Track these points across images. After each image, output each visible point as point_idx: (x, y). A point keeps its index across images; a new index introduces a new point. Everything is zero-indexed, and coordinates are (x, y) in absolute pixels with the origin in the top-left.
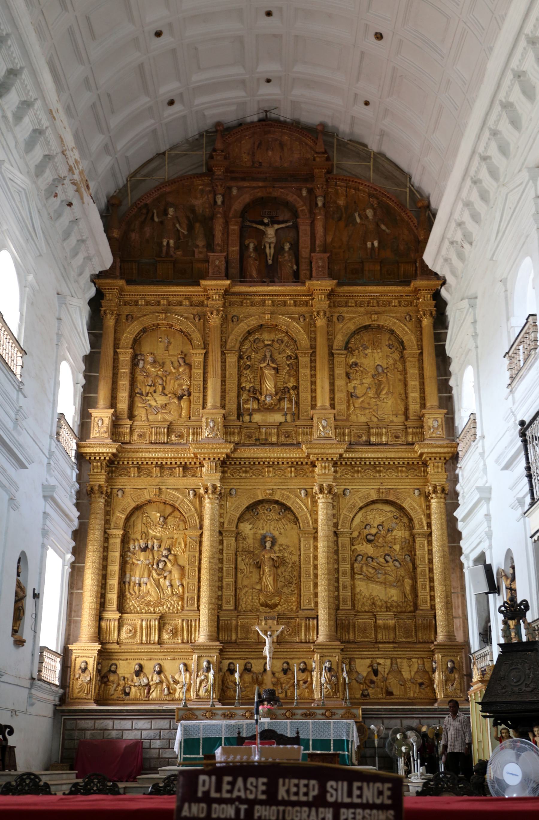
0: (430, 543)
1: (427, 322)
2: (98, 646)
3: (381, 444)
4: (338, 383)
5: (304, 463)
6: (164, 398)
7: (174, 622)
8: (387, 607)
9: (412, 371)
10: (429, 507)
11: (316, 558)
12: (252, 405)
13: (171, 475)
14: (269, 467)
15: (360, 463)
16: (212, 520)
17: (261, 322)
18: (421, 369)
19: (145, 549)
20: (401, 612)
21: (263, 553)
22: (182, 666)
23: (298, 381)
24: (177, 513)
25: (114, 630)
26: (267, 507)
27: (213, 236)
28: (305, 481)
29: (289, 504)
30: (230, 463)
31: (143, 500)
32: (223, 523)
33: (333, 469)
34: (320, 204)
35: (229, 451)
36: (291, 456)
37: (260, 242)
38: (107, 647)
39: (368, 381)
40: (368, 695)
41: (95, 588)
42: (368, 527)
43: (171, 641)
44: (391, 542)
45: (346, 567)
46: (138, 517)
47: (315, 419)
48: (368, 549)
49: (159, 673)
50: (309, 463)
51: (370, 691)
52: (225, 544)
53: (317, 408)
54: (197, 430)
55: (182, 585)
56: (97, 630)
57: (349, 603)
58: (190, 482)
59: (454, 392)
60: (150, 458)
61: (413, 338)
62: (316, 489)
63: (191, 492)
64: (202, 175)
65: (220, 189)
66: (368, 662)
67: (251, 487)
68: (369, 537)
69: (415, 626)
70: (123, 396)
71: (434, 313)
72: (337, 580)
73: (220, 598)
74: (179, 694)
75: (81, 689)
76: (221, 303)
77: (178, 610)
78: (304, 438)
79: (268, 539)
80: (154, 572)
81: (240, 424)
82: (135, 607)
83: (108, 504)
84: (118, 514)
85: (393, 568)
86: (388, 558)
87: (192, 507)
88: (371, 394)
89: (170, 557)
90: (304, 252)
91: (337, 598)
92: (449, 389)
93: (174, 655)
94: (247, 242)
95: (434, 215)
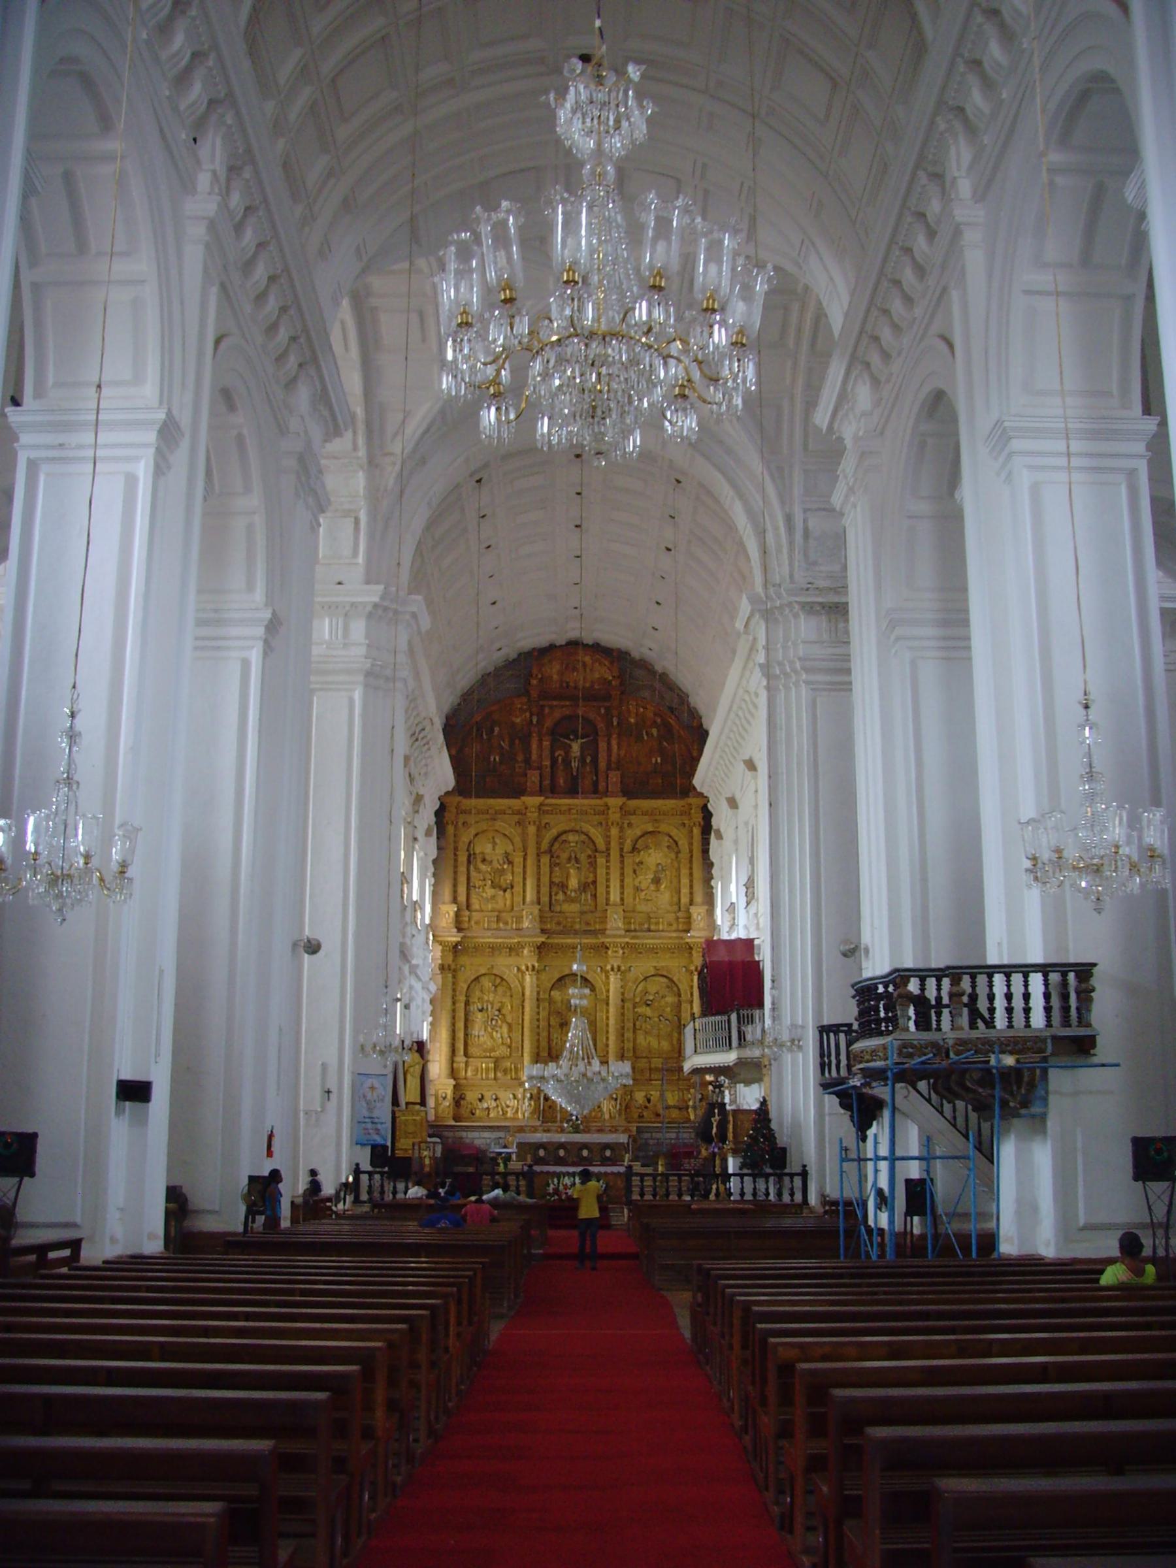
1: (697, 831)
2: (452, 1082)
3: (658, 931)
4: (626, 880)
6: (493, 890)
11: (607, 1018)
12: (561, 896)
16: (531, 992)
17: (568, 829)
18: (691, 868)
19: (481, 1011)
22: (511, 1096)
23: (596, 877)
24: (504, 983)
27: (530, 753)
33: (621, 952)
34: (615, 723)
35: (543, 940)
40: (643, 1116)
47: (609, 912)
51: (645, 1114)
53: (611, 903)
54: (519, 919)
58: (512, 960)
59: (714, 891)
62: (609, 967)
66: (643, 1094)
68: (649, 1002)
70: (462, 889)
71: (702, 823)
72: (623, 1035)
73: (538, 1047)
74: (509, 1115)
76: (536, 814)
83: (454, 977)
90: (602, 765)
92: (712, 888)
93: (507, 1087)
94: (557, 754)
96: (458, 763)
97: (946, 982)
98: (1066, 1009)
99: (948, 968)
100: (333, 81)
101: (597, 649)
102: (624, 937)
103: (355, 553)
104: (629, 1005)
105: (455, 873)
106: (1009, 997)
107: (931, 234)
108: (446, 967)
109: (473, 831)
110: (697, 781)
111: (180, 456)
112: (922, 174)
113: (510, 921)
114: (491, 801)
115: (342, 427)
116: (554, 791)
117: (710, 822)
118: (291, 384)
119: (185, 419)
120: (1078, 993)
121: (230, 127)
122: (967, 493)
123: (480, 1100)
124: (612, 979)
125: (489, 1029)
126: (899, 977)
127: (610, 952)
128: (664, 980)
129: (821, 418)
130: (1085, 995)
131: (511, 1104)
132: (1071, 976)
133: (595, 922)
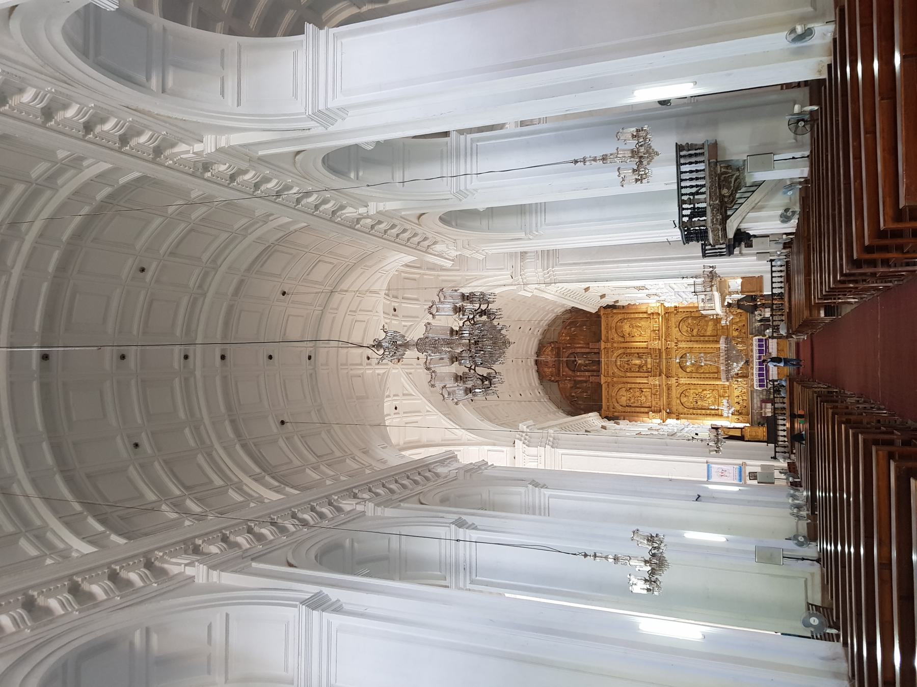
0: (693, 312)
1: (615, 311)
9: (632, 316)
10: (681, 312)
11: (699, 348)
12: (645, 368)
17: (614, 365)
18: (631, 313)
19: (697, 402)
27: (582, 380)
33: (669, 342)
37: (583, 365)
39: (635, 330)
45: (702, 338)
48: (695, 332)
49: (738, 397)
61: (619, 316)
62: (676, 347)
64: (559, 385)
65: (565, 378)
66: (734, 332)
70: (642, 410)
73: (713, 378)
75: (744, 420)
76: (609, 378)
83: (682, 414)
84: (685, 411)
88: (640, 329)
90: (587, 350)
95: (573, 307)
96: (587, 411)
97: (685, 206)
98: (696, 155)
99: (679, 205)
100: (318, 457)
101: (538, 353)
102: (662, 341)
103: (503, 451)
104: (693, 339)
105: (635, 412)
106: (691, 179)
107: (380, 222)
108: (677, 417)
109: (616, 404)
110: (594, 312)
111: (469, 519)
112: (356, 227)
114: (603, 397)
115: (452, 455)
116: (599, 371)
117: (611, 305)
118: (437, 475)
119: (456, 517)
120: (689, 150)
121: (339, 497)
122: (481, 207)
123: (739, 403)
126: (682, 226)
127: (669, 347)
128: (681, 324)
129: (448, 264)
130: (689, 147)
131: (740, 390)
132: (682, 153)
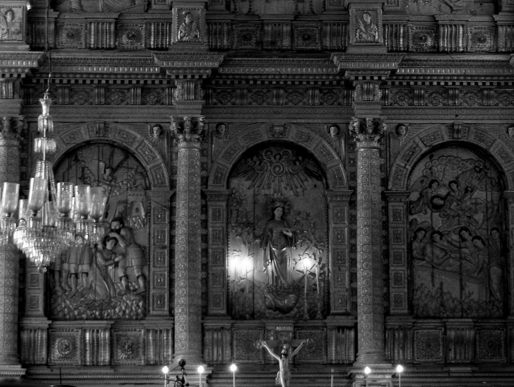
3: (456, 52)
5: (335, 83)
7: (133, 333)
8: (462, 310)
11: (353, 234)
13: (122, 101)
14: (278, 87)
15: (423, 84)
20: (484, 318)
21: (270, 225)
24: (131, 162)
25: (41, 345)
26: (275, 152)
28: (335, 111)
29: (311, 148)
30: (217, 82)
31: (79, 141)
32: (207, 178)
33: (380, 94)
35: (216, 65)
36: (315, 71)
38: (32, 371)
41: (12, 282)
42: (435, 185)
43: (129, 362)
44: (470, 209)
46: (70, 167)
47: (352, 11)
50: (343, 83)
52: (210, 212)
55: (143, 276)
56: (16, 346)
57: (405, 304)
60: (89, 74)
63: (155, 129)
67: (249, 121)
69: (506, 339)
72: (386, 269)
77: (137, 314)
78: (334, 42)
79: (278, 204)
80: (98, 255)
81: (232, 17)
82: (70, 310)
85: (473, 249)
86: (465, 234)
87: (156, 153)
89: (123, 232)
91: (386, 297)
113: (143, 33)
124: (361, 147)
125: (100, 260)
127: (355, 94)
128: (466, 155)
133: (323, 34)
